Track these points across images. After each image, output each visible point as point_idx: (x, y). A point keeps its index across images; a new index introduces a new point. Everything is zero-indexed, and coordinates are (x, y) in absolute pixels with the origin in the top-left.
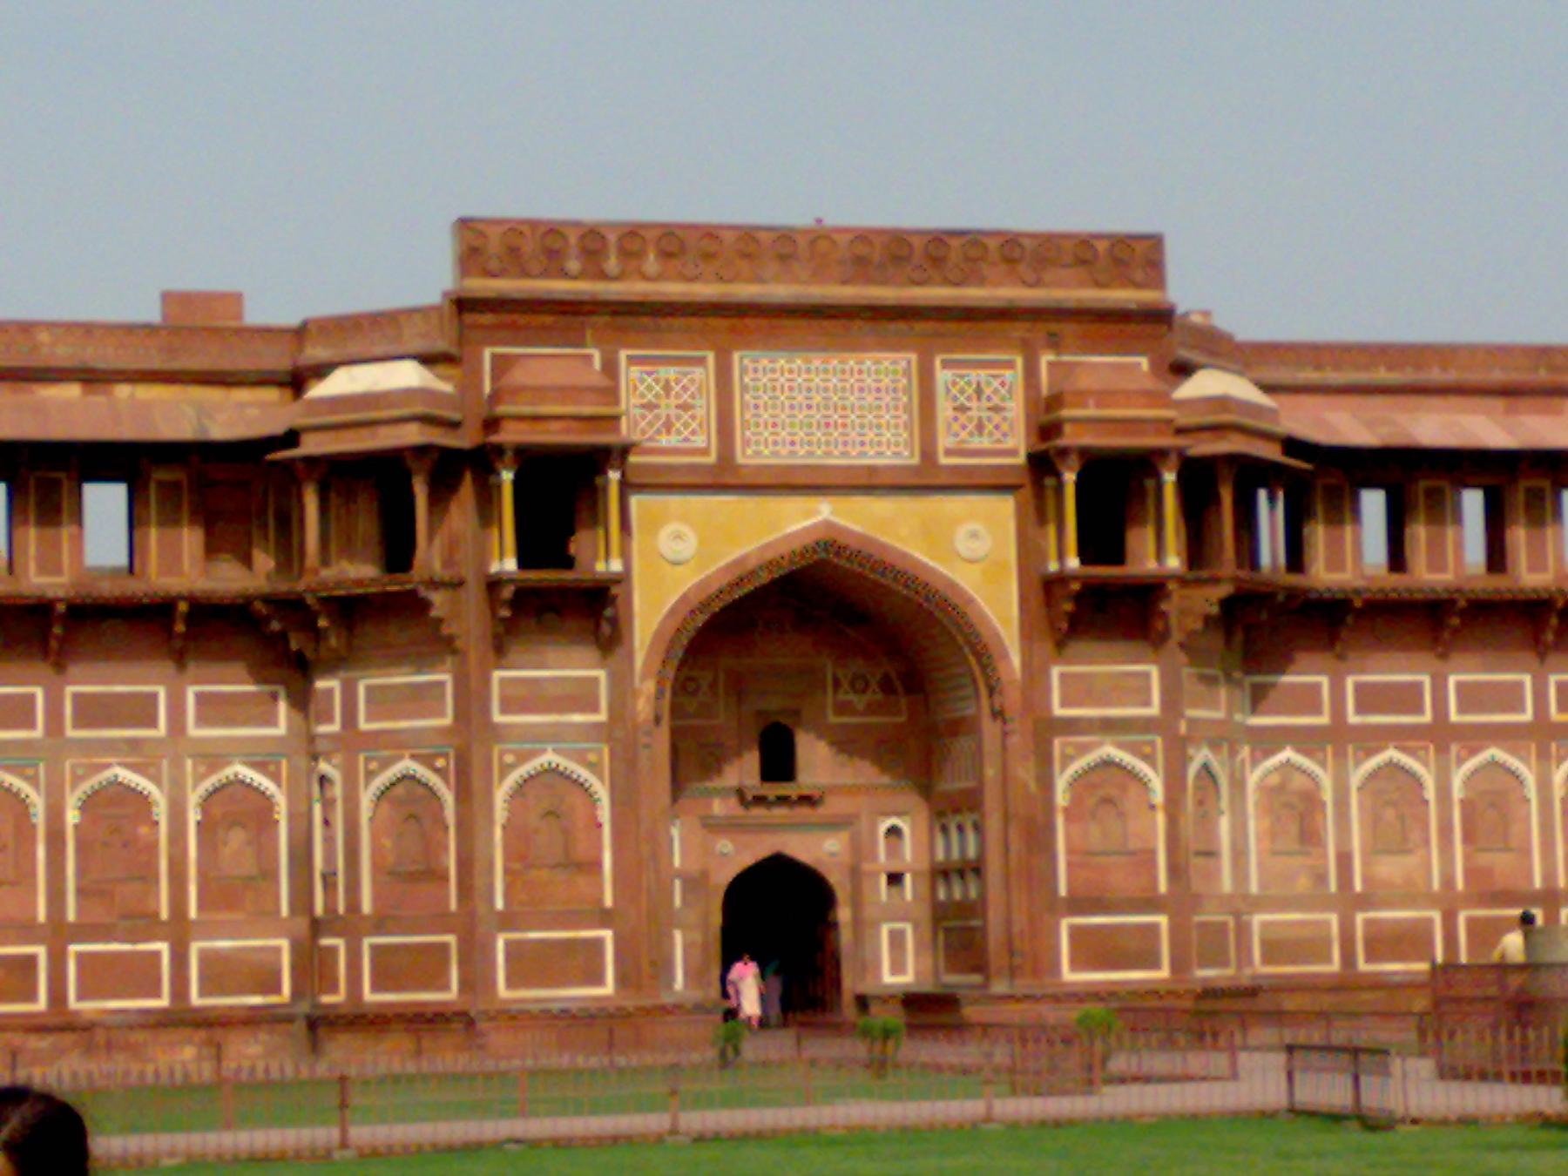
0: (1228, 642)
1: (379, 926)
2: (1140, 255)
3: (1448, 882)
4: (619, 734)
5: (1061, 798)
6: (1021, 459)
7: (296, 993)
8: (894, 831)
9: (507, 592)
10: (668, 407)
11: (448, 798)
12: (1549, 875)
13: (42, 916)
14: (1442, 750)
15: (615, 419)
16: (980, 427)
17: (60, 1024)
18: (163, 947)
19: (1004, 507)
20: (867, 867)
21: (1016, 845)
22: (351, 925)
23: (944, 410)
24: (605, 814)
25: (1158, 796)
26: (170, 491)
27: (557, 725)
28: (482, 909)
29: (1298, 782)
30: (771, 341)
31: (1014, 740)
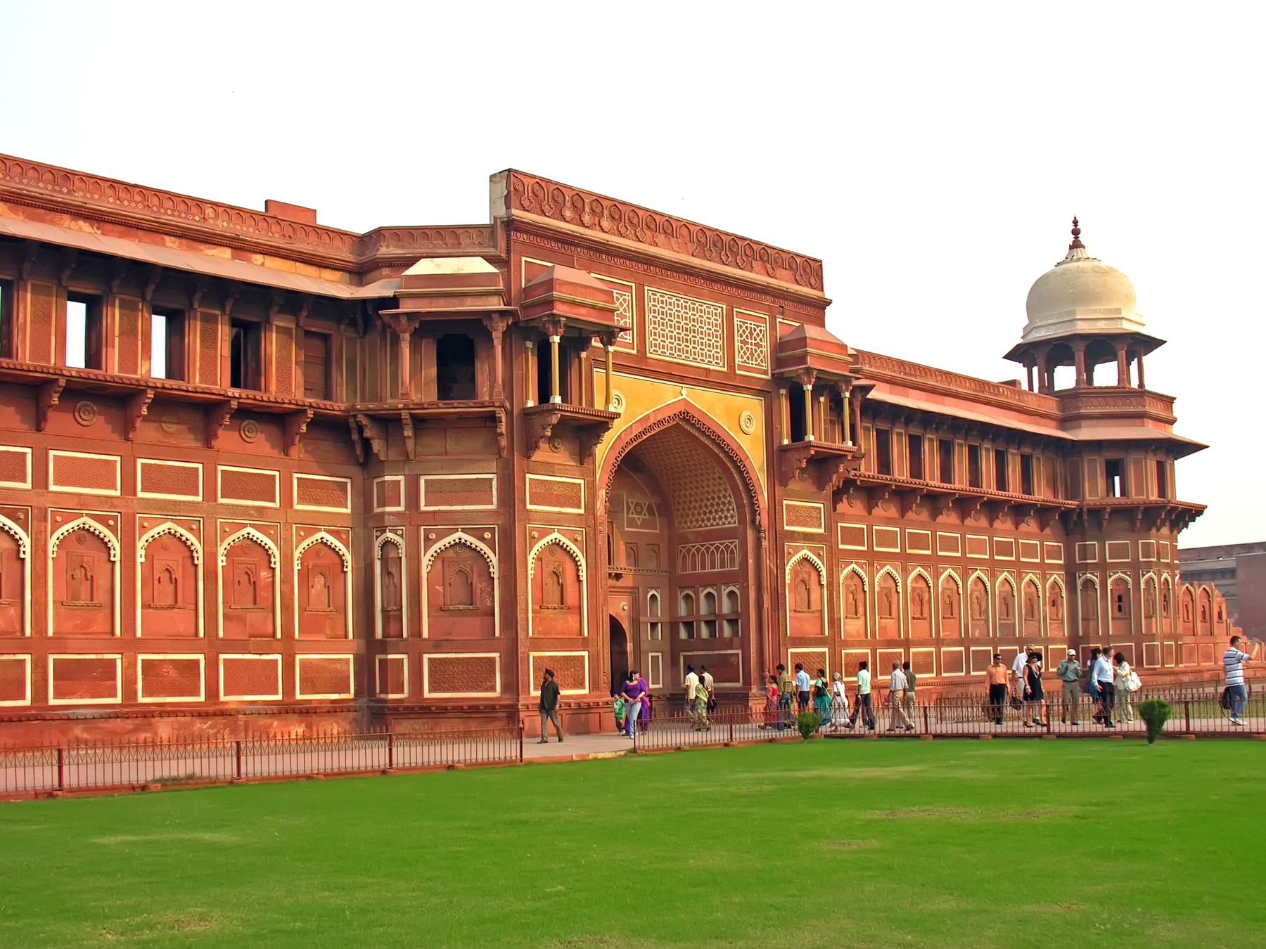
1: (437, 646)
3: (873, 635)
5: (788, 578)
6: (769, 377)
7: (358, 693)
8: (653, 596)
9: (554, 420)
11: (494, 559)
12: (907, 632)
13: (201, 634)
15: (612, 311)
17: (213, 712)
18: (278, 657)
20: (642, 619)
22: (416, 648)
25: (824, 582)
27: (560, 513)
28: (521, 635)
30: (660, 283)
31: (765, 543)
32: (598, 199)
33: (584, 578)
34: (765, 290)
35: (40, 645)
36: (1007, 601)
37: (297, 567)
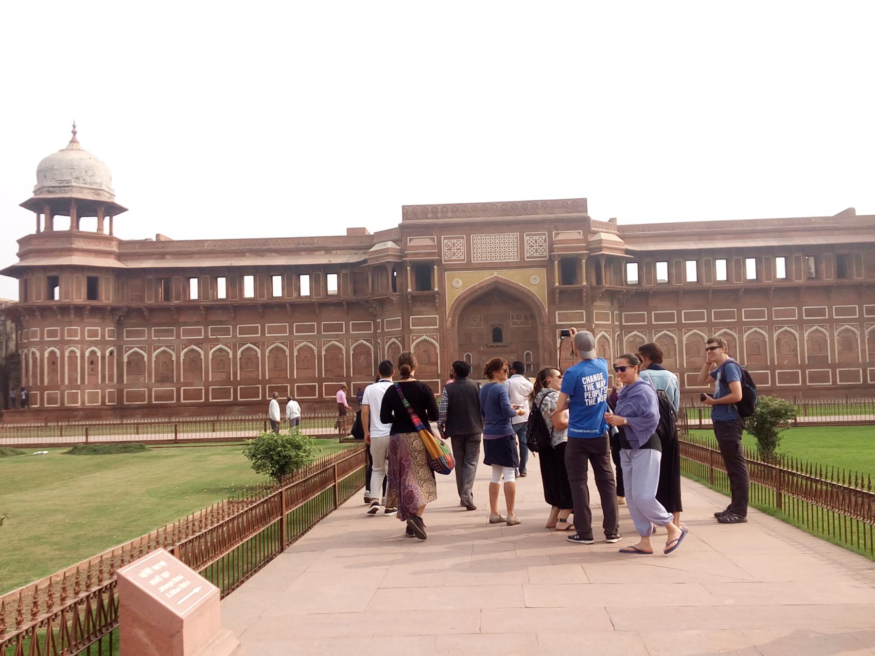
0: (612, 304)
2: (580, 204)
3: (682, 365)
4: (441, 330)
9: (409, 297)
10: (454, 250)
14: (680, 330)
16: (536, 251)
19: (544, 270)
21: (547, 357)
23: (526, 247)
24: (438, 351)
26: (345, 275)
29: (639, 340)
32: (445, 206)
33: (438, 351)
34: (542, 222)
35: (264, 382)
36: (818, 343)
37: (351, 353)
